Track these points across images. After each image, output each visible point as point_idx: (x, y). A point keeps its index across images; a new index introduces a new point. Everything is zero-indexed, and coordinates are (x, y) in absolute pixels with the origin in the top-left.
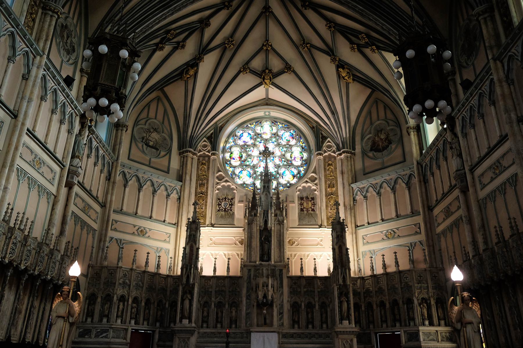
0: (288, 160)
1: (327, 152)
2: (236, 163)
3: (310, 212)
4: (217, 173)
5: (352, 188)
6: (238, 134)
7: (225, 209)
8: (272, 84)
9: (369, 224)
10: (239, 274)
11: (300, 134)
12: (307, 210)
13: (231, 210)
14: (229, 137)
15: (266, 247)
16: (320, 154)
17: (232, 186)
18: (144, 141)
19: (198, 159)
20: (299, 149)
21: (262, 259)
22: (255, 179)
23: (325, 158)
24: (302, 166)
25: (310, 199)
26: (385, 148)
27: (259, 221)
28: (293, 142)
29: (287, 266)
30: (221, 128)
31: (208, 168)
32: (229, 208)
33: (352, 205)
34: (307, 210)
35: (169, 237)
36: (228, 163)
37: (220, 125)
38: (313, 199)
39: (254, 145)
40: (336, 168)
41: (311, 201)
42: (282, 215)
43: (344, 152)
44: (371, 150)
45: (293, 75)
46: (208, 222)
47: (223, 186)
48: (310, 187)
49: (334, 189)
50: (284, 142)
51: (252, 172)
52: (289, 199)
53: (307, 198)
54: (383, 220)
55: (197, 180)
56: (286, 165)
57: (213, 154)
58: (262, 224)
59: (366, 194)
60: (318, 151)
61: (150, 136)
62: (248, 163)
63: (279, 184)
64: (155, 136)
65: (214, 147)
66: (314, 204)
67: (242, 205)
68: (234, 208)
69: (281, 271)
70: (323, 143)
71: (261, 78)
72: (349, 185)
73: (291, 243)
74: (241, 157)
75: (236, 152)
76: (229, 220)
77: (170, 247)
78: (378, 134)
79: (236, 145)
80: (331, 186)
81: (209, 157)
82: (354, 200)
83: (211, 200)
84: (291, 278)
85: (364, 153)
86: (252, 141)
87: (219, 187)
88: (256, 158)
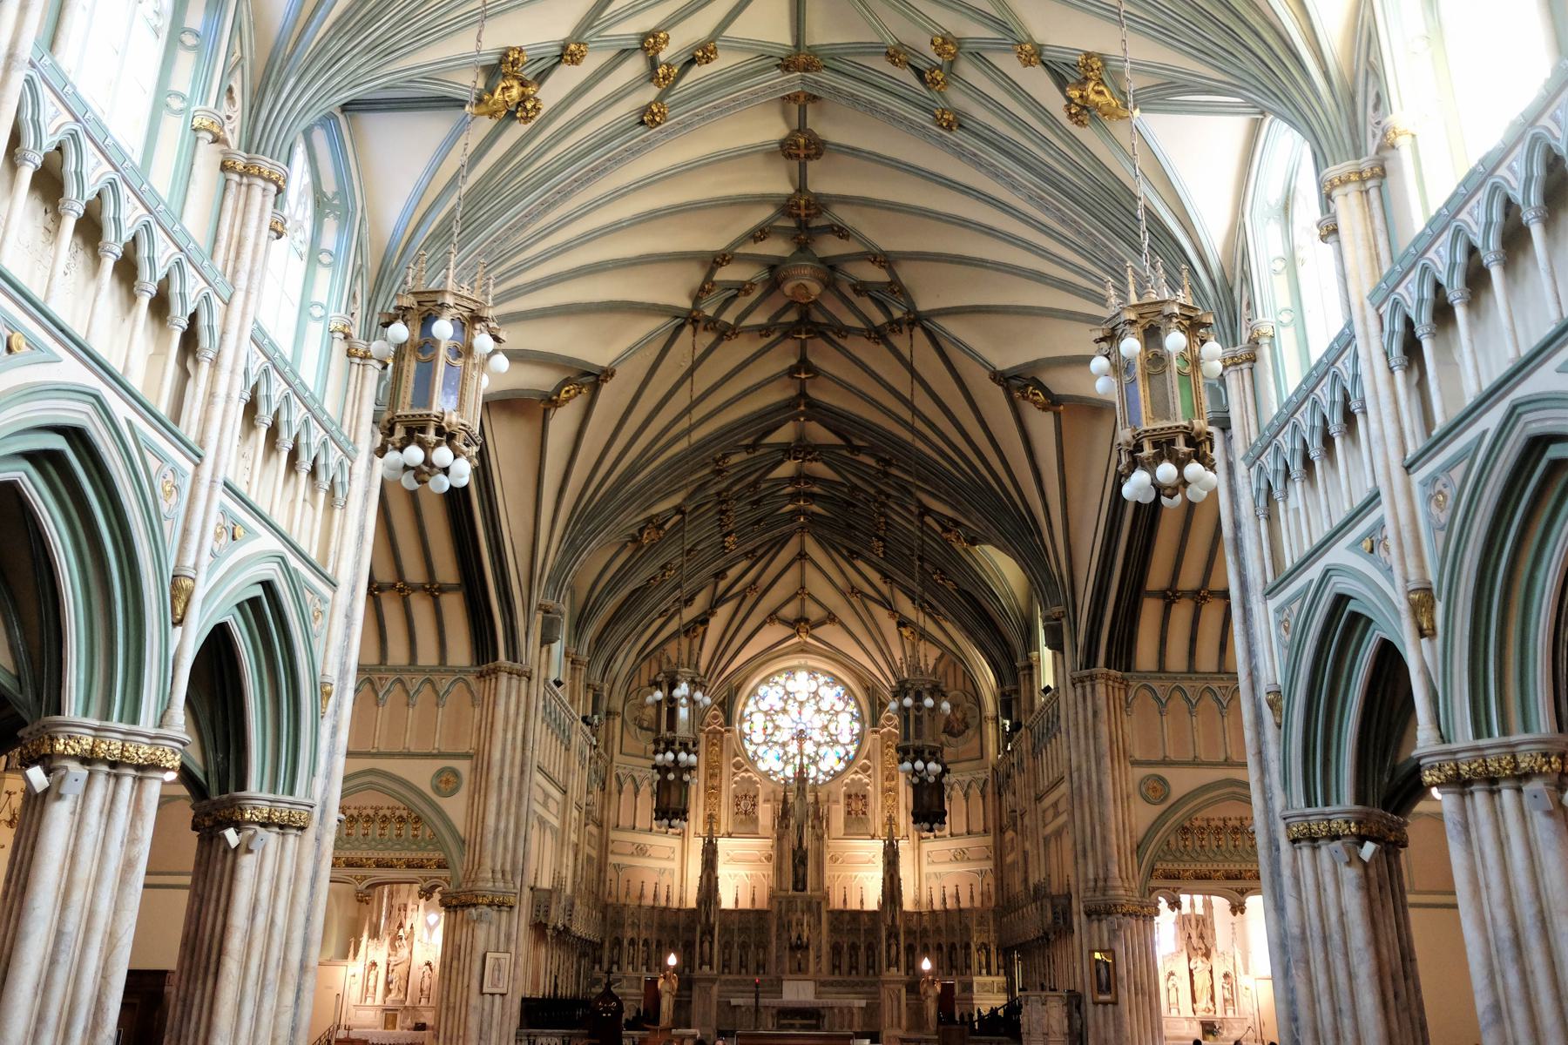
2: (758, 737)
3: (860, 815)
10: (765, 907)
11: (850, 693)
12: (857, 814)
14: (748, 697)
15: (801, 872)
16: (876, 732)
20: (849, 717)
21: (795, 888)
22: (786, 763)
24: (852, 742)
26: (961, 733)
27: (792, 835)
28: (839, 706)
29: (826, 897)
30: (739, 688)
31: (721, 750)
34: (857, 814)
39: (784, 711)
45: (837, 627)
46: (722, 831)
47: (743, 778)
48: (860, 780)
50: (825, 706)
51: (781, 752)
52: (833, 798)
53: (857, 795)
54: (952, 835)
57: (729, 731)
58: (796, 843)
63: (819, 770)
65: (729, 721)
67: (768, 806)
69: (819, 903)
70: (881, 713)
73: (834, 859)
74: (765, 729)
75: (759, 720)
76: (752, 827)
77: (676, 865)
80: (890, 778)
81: (722, 734)
83: (726, 798)
84: (832, 912)
86: (782, 704)
87: (737, 779)
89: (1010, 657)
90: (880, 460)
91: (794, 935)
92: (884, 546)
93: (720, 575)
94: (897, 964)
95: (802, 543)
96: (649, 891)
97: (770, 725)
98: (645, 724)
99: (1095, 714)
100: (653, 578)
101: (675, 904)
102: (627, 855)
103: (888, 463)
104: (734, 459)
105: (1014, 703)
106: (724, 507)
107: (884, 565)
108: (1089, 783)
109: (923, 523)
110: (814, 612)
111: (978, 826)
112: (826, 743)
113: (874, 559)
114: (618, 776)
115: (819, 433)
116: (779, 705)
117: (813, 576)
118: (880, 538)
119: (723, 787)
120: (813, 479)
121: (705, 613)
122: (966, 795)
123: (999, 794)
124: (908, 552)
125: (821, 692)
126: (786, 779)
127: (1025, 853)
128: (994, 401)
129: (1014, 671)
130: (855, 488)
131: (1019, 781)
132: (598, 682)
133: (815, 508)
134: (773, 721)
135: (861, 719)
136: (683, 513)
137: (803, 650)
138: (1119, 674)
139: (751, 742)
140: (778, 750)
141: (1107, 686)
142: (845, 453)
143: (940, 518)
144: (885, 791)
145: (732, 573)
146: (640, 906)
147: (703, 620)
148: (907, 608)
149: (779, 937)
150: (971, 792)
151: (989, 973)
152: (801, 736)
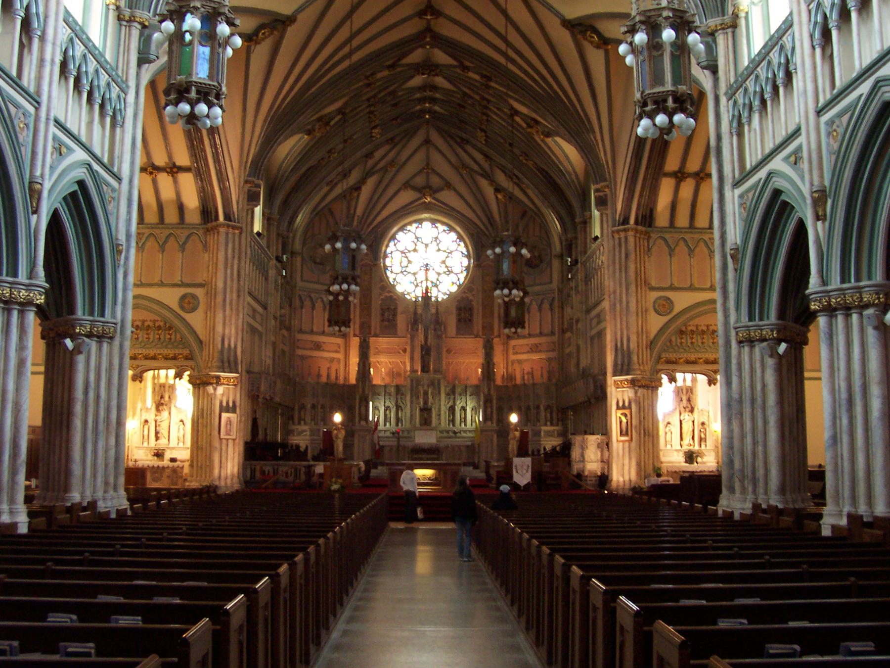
11: (460, 237)
14: (389, 241)
21: (423, 370)
22: (417, 286)
26: (537, 266)
27: (421, 337)
35: (339, 347)
39: (415, 250)
42: (440, 330)
45: (452, 193)
46: (373, 333)
47: (386, 296)
63: (439, 291)
75: (397, 256)
89: (572, 216)
90: (483, 76)
91: (421, 401)
92: (486, 136)
93: (369, 155)
94: (491, 420)
95: (428, 132)
96: (324, 373)
97: (405, 262)
98: (318, 260)
99: (627, 256)
100: (322, 159)
101: (341, 381)
102: (307, 349)
103: (489, 79)
104: (379, 75)
105: (574, 246)
106: (372, 108)
107: (485, 149)
108: (621, 301)
109: (513, 120)
110: (435, 181)
111: (547, 329)
113: (479, 145)
114: (299, 295)
115: (441, 57)
117: (436, 157)
118: (482, 130)
120: (434, 88)
121: (359, 182)
122: (540, 310)
123: (562, 308)
124: (502, 141)
126: (417, 297)
127: (578, 347)
128: (563, 38)
129: (574, 225)
130: (465, 94)
131: (575, 299)
132: (285, 233)
133: (437, 108)
135: (468, 256)
136: (344, 114)
137: (427, 208)
138: (643, 229)
139: (392, 272)
140: (411, 278)
141: (635, 237)
142: (458, 70)
143: (524, 117)
144: (484, 306)
145: (378, 154)
146: (318, 383)
147: (357, 188)
148: (501, 178)
150: (544, 306)
151: (552, 425)
152: (427, 267)
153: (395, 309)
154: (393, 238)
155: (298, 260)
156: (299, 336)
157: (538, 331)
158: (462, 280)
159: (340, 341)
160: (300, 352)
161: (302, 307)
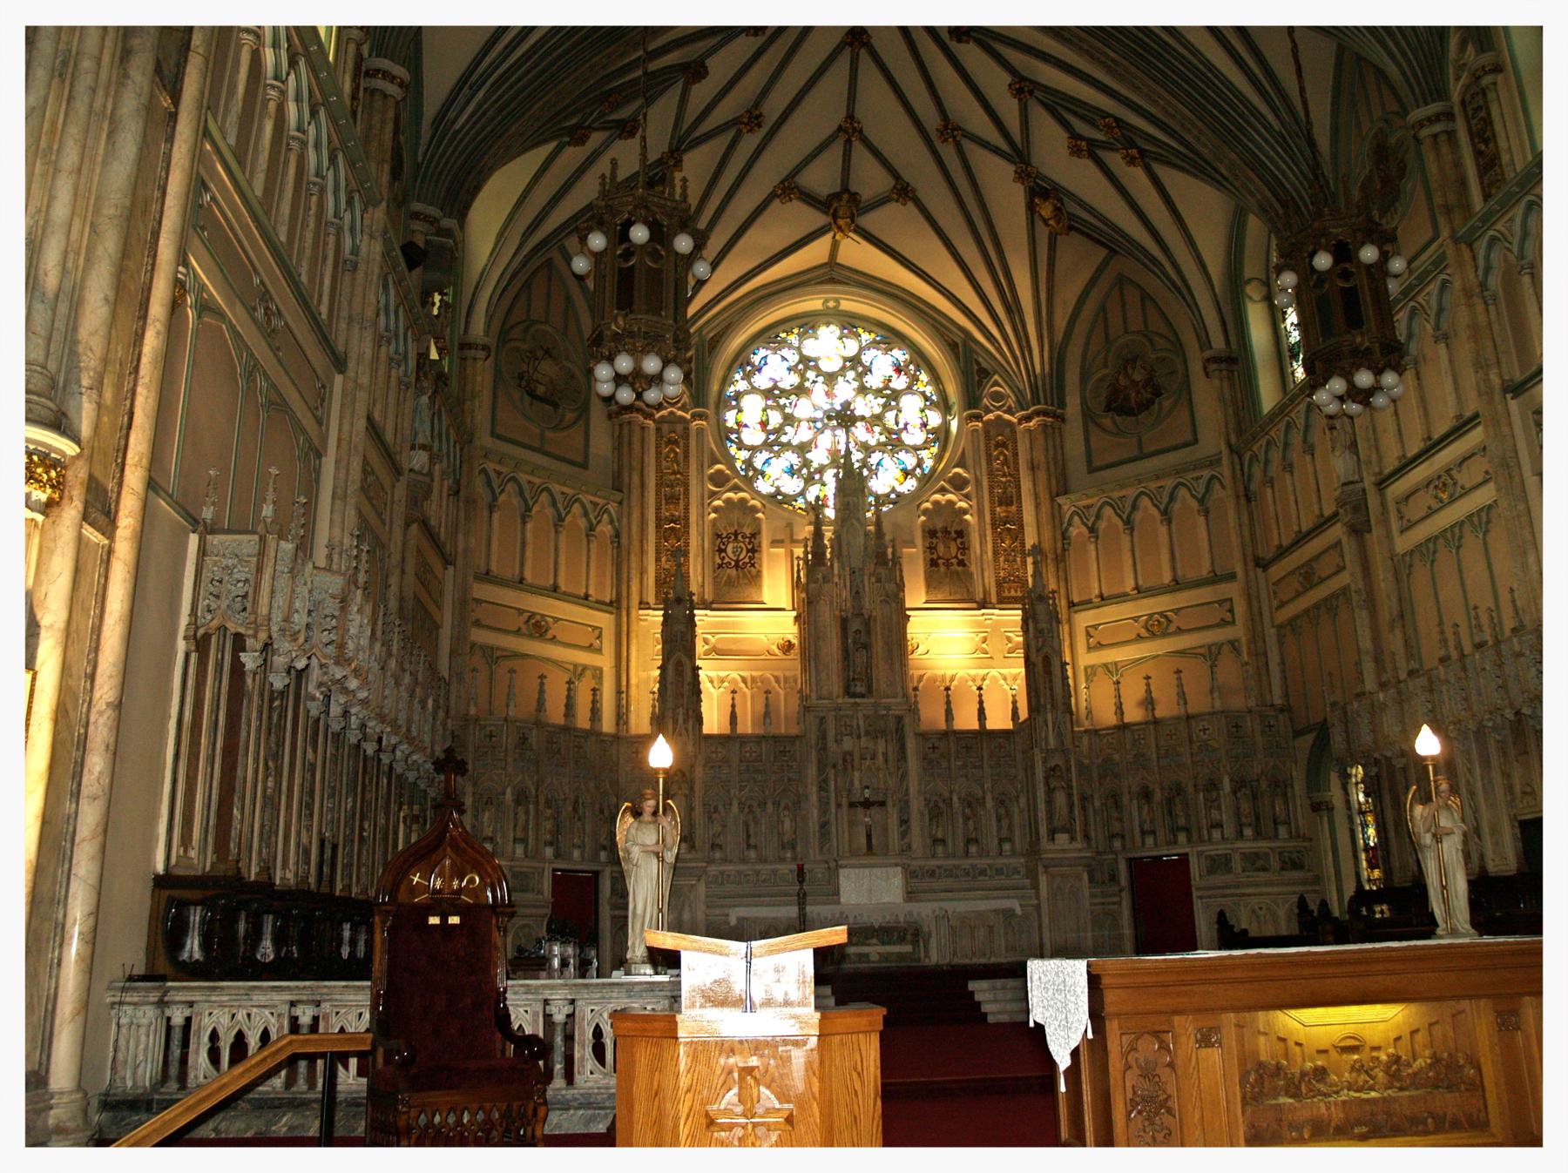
0: (890, 432)
1: (992, 411)
2: (753, 436)
3: (956, 567)
4: (710, 466)
5: (1060, 505)
6: (756, 359)
7: (737, 562)
8: (855, 231)
9: (1103, 599)
11: (920, 359)
13: (753, 565)
14: (730, 369)
16: (978, 418)
17: (753, 502)
18: (524, 383)
19: (658, 430)
20: (918, 402)
22: (810, 480)
23: (987, 424)
24: (925, 446)
25: (954, 535)
28: (900, 383)
32: (747, 560)
33: (1059, 551)
34: (948, 565)
35: (599, 637)
36: (733, 437)
37: (711, 335)
38: (960, 534)
40: (1015, 455)
41: (955, 540)
43: (1038, 413)
44: (1108, 409)
47: (728, 501)
48: (951, 503)
49: (1013, 508)
50: (874, 381)
53: (946, 531)
55: (659, 486)
56: (885, 445)
57: (695, 417)
59: (1094, 524)
60: (970, 408)
61: (535, 370)
62: (784, 439)
64: (547, 368)
66: (964, 549)
68: (760, 559)
71: (826, 213)
72: (1052, 500)
75: (753, 407)
77: (605, 662)
78: (1125, 369)
79: (754, 390)
82: (1064, 536)
85: (1088, 416)
86: (794, 379)
87: (718, 503)
88: (804, 425)
97: (775, 419)
102: (507, 632)
112: (881, 446)
116: (793, 380)
119: (693, 518)
125: (866, 358)
134: (782, 408)
135: (944, 406)
139: (741, 446)
149: (823, 786)
151: (1258, 835)
153: (755, 535)
154: (740, 360)
155: (482, 374)
156: (482, 591)
157: (1167, 578)
158: (928, 463)
159: (604, 620)
160: (479, 636)
161: (491, 508)
